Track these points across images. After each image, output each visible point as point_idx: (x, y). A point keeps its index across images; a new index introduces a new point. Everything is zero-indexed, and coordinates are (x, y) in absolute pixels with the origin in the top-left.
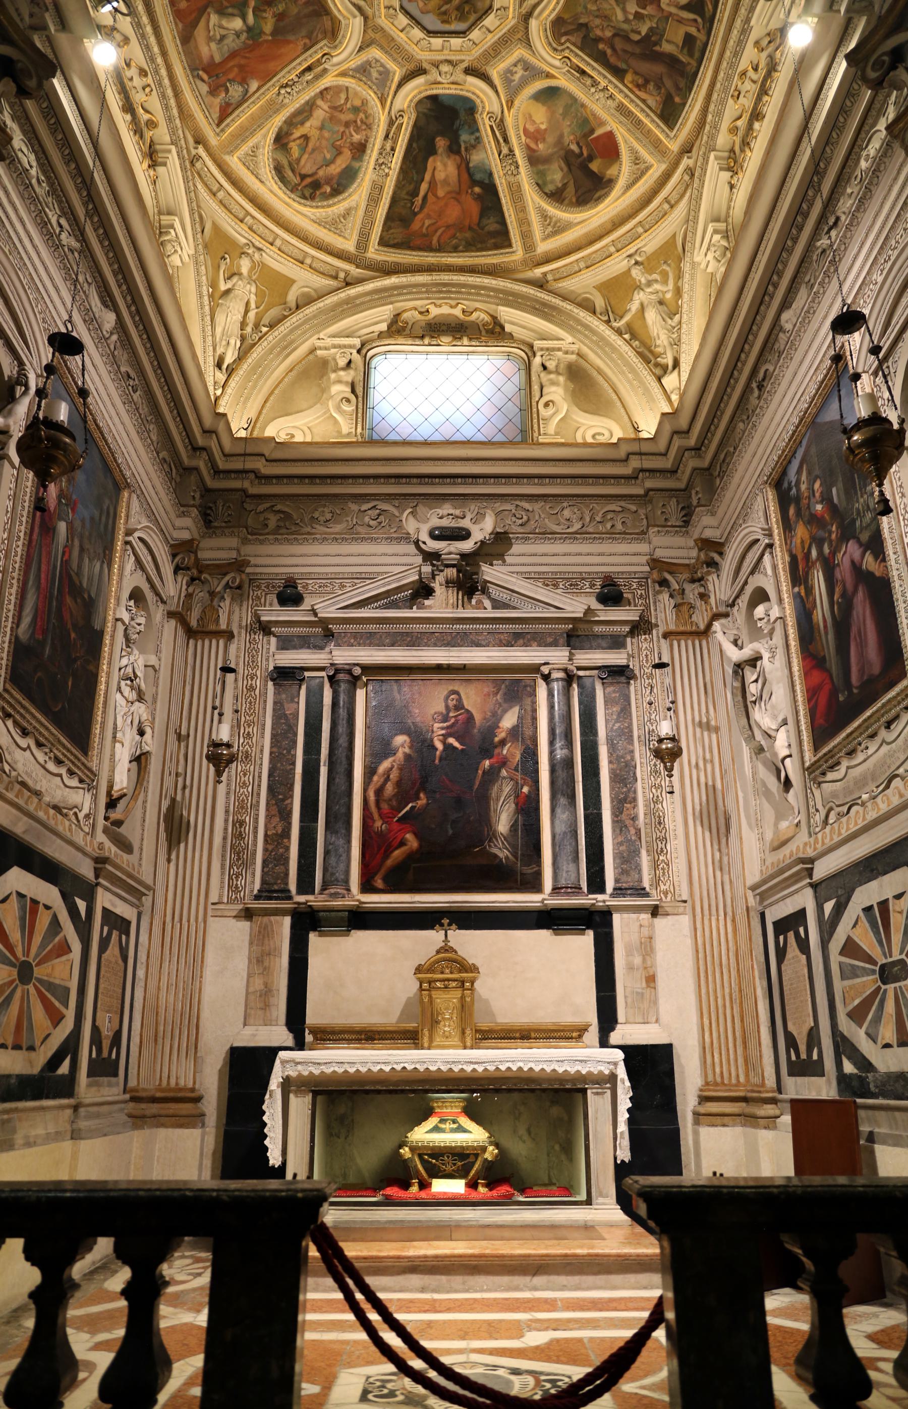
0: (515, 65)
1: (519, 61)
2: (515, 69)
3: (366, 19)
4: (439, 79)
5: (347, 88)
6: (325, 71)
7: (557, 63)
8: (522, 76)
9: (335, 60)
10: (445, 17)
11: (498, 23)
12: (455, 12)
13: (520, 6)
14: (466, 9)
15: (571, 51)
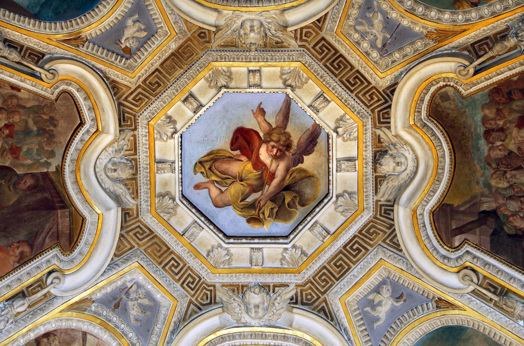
0: (377, 290)
1: (383, 283)
2: (378, 298)
3: (126, 214)
4: (246, 318)
5: (85, 334)
6: (50, 299)
7: (453, 280)
8: (393, 311)
9: (69, 282)
10: (253, 213)
11: (342, 219)
12: (270, 205)
13: (376, 192)
14: (288, 200)
15: (475, 257)
